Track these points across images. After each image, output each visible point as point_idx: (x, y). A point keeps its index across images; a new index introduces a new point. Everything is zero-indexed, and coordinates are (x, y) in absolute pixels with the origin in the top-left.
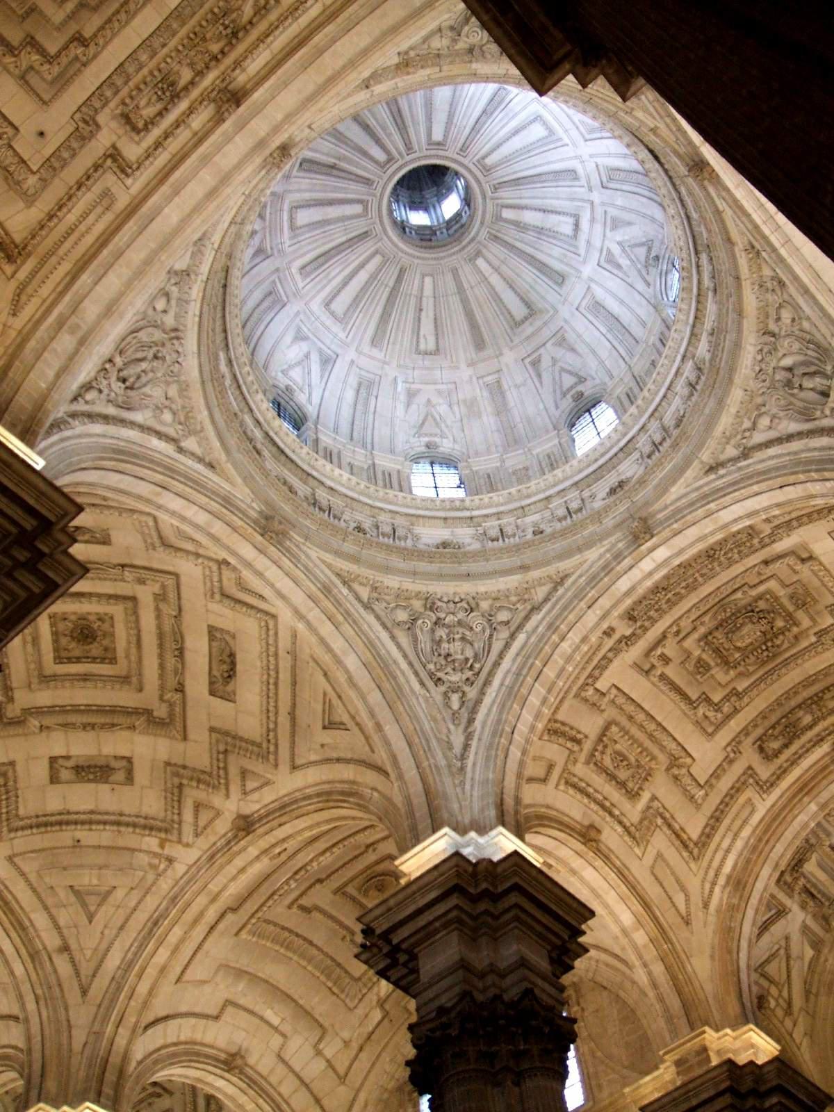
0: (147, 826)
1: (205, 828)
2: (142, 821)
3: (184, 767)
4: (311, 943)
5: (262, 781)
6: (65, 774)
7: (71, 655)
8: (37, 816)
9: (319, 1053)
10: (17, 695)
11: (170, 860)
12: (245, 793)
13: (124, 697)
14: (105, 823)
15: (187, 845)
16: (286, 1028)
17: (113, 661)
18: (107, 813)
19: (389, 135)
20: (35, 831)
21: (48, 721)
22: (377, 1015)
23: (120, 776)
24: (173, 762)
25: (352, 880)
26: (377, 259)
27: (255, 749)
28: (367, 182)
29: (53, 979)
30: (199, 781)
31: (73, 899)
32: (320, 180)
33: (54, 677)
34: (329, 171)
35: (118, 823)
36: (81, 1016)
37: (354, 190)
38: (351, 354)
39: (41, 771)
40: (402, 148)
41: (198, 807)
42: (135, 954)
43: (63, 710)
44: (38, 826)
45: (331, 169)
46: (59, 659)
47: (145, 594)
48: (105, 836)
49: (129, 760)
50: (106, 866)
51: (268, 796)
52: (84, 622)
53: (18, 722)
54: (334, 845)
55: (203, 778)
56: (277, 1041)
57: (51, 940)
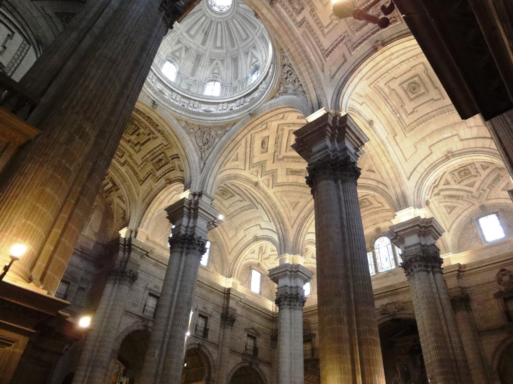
4: (428, 113)
16: (454, 133)
19: (197, 16)
26: (234, 21)
28: (212, 21)
29: (382, 191)
32: (209, 38)
34: (207, 35)
37: (214, 26)
38: (256, 38)
40: (200, 13)
45: (206, 34)
56: (456, 138)
57: (375, 183)
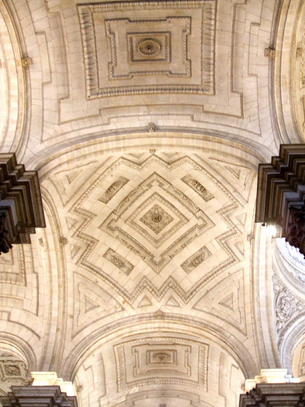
0: (124, 293)
1: (143, 306)
2: (123, 290)
3: (150, 282)
4: (125, 362)
5: (177, 304)
6: (109, 256)
7: (146, 221)
8: (91, 264)
9: (99, 401)
10: (120, 220)
11: (123, 309)
12: (166, 305)
13: (149, 247)
14: (111, 282)
15: (133, 308)
16: (96, 386)
17: (157, 233)
18: (113, 279)
20: (88, 269)
21: (121, 236)
22: (124, 399)
23: (125, 269)
24: (147, 277)
25: (153, 351)
27: (183, 293)
30: (153, 290)
31: (84, 301)
33: (135, 224)
35: (115, 285)
36: (69, 346)
39: (103, 250)
41: (146, 297)
42: (96, 335)
43: (127, 236)
44: (90, 268)
46: (141, 220)
47: (194, 221)
48: (106, 286)
49: (133, 267)
50: (100, 297)
51: (176, 311)
52: (162, 214)
53: (112, 230)
54: (168, 337)
55: (153, 290)
57: (69, 310)
